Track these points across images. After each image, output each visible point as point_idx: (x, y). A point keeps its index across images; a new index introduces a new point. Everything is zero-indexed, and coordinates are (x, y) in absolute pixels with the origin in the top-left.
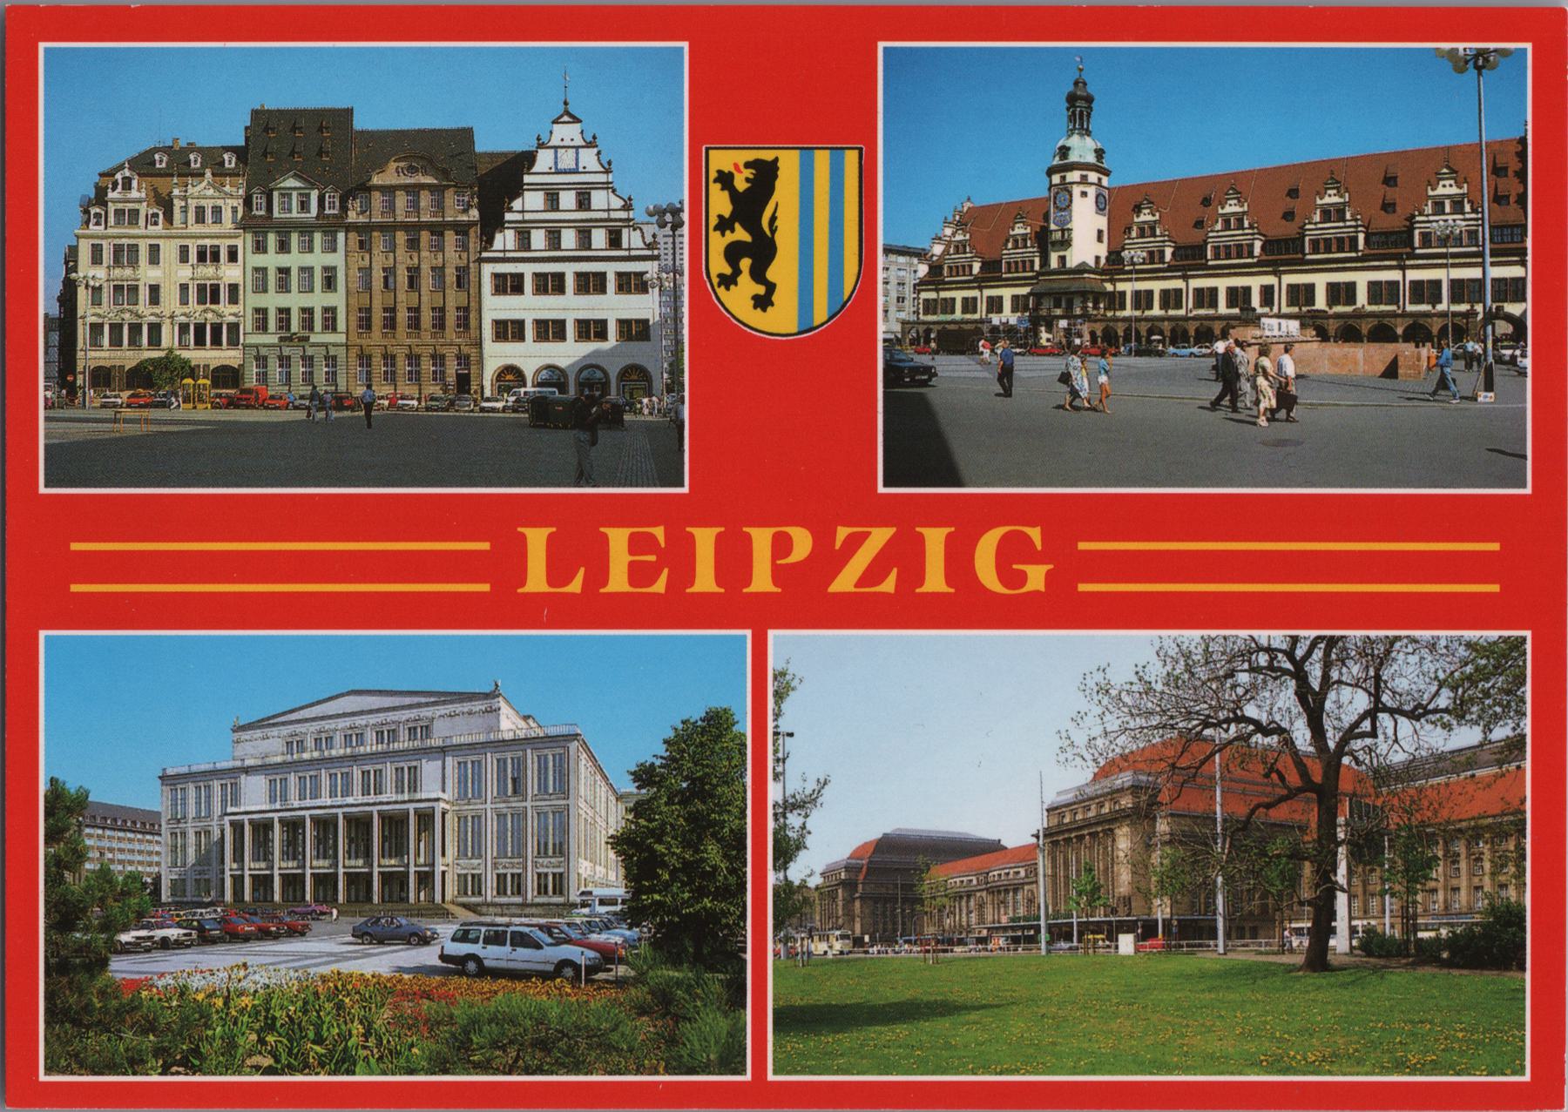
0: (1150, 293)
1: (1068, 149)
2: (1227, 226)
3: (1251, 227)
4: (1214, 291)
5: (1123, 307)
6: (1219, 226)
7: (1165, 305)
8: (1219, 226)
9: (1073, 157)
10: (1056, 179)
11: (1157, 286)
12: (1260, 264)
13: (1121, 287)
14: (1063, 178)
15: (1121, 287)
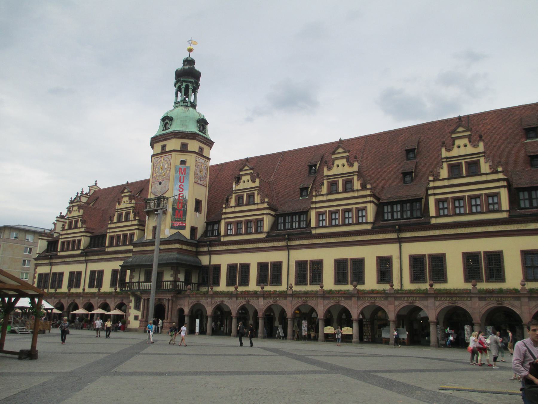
0: (246, 267)
1: (171, 119)
2: (333, 188)
3: (364, 187)
4: (318, 264)
5: (217, 282)
6: (325, 189)
7: (262, 280)
8: (325, 189)
9: (175, 127)
10: (158, 147)
11: (254, 259)
12: (377, 228)
13: (216, 260)
14: (164, 147)
15: (216, 260)
